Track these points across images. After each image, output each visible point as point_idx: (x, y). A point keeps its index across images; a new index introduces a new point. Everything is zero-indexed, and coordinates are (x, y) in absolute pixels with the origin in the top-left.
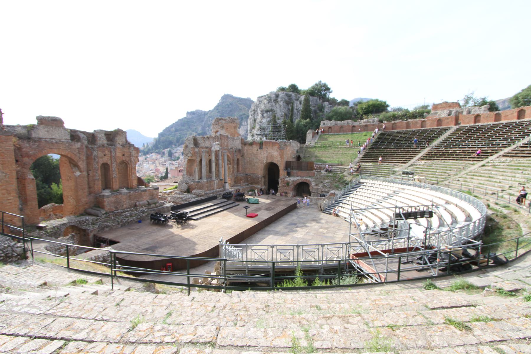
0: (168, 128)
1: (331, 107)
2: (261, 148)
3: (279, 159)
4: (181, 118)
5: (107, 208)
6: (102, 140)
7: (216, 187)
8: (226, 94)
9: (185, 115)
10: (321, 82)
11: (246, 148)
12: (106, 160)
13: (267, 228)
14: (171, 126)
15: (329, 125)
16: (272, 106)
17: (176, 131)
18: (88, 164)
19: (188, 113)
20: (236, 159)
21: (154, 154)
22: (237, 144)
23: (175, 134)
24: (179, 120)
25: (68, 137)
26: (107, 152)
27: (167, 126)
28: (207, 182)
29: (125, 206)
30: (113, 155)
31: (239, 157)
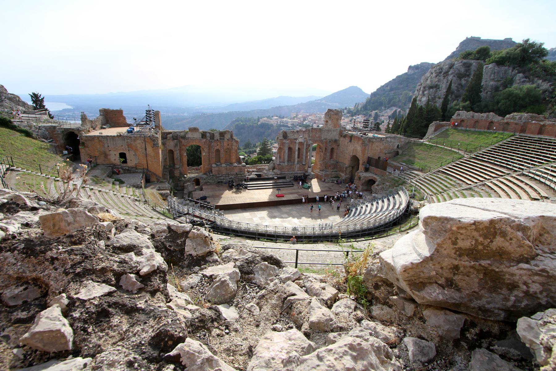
0: (383, 86)
2: (351, 141)
3: (361, 154)
4: (400, 74)
5: (214, 173)
6: (217, 137)
7: (296, 170)
8: (469, 37)
9: (406, 71)
10: (528, 40)
11: (342, 139)
12: (218, 147)
13: (280, 207)
14: (387, 85)
15: (464, 117)
16: (439, 81)
17: (392, 89)
18: (209, 149)
19: (410, 67)
20: (330, 148)
21: (360, 116)
22: (334, 135)
23: (389, 94)
24: (398, 77)
25: (201, 136)
27: (383, 84)
28: (288, 165)
31: (334, 146)
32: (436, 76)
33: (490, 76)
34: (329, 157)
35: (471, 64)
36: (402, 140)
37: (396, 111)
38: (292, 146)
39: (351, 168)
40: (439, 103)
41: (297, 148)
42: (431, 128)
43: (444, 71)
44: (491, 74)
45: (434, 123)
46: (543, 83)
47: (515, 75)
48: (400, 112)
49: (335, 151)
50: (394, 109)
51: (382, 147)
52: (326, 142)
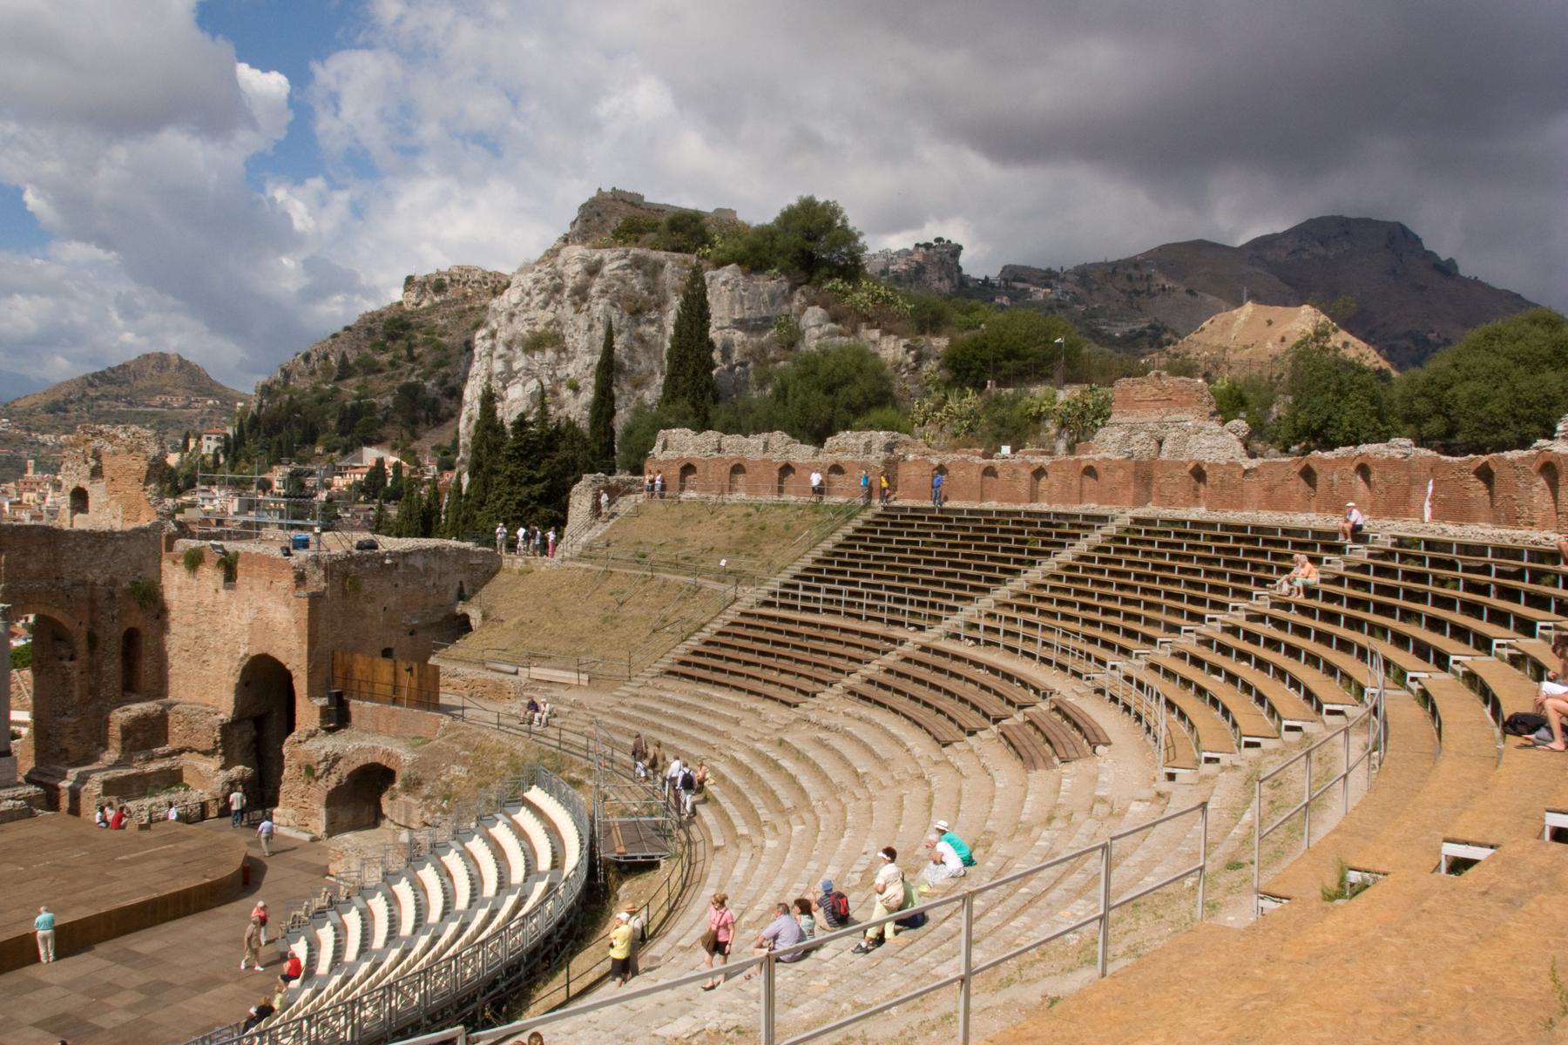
1: (831, 333)
15: (689, 453)
31: (136, 619)
32: (547, 304)
33: (732, 310)
34: (116, 684)
35: (660, 266)
36: (474, 561)
37: (380, 462)
39: (249, 725)
40: (576, 408)
42: (580, 501)
43: (570, 284)
44: (732, 303)
45: (588, 478)
46: (885, 340)
47: (803, 310)
48: (397, 468)
49: (147, 644)
50: (370, 455)
51: (392, 600)
52: (92, 601)
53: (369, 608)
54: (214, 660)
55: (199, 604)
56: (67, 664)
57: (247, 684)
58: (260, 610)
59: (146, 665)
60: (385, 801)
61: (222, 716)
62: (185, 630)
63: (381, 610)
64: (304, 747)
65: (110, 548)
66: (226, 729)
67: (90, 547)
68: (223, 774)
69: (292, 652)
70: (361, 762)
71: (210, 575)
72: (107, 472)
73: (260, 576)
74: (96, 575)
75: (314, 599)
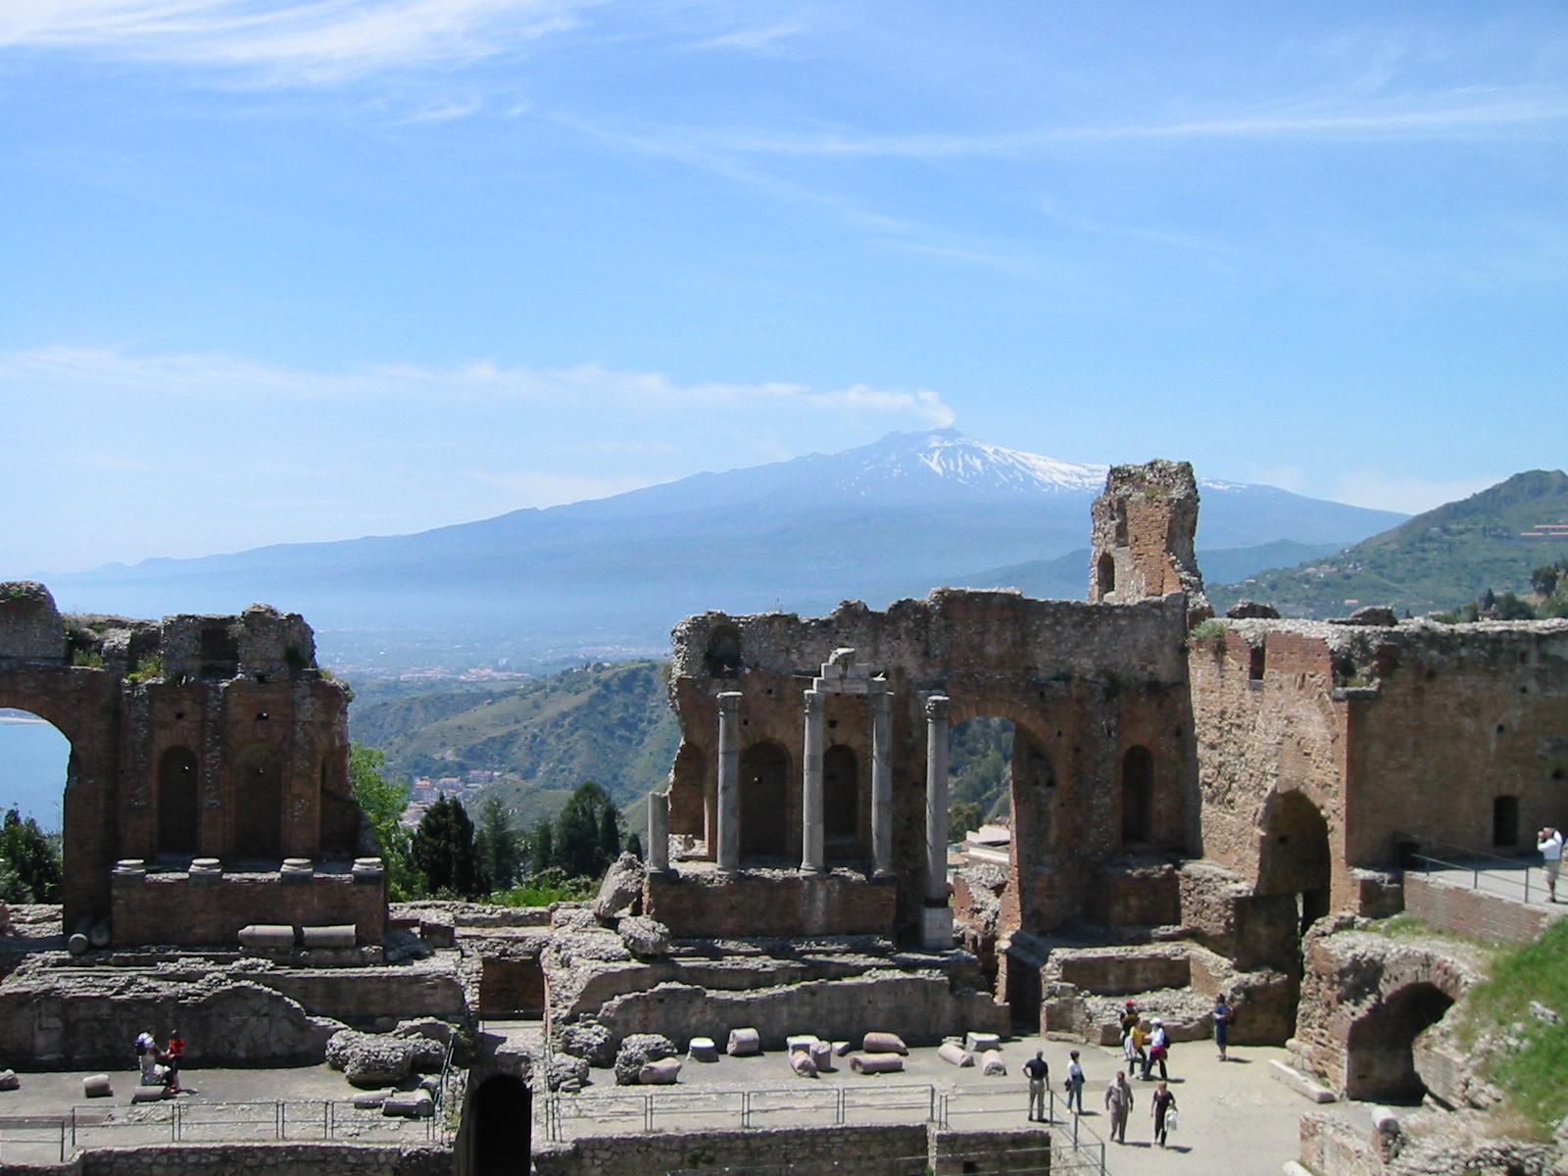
26: (186, 705)
29: (199, 931)
30: (211, 716)
31: (1144, 733)
38: (781, 734)
41: (810, 745)
51: (1514, 716)
53: (1469, 724)
54: (1240, 798)
55: (1223, 713)
56: (1044, 791)
57: (1283, 840)
58: (1289, 720)
59: (1161, 802)
60: (1418, 1053)
61: (1242, 886)
62: (1209, 753)
63: (1492, 730)
64: (1324, 943)
65: (1105, 629)
66: (1241, 906)
67: (1076, 626)
68: (1238, 977)
69: (1329, 792)
70: (1408, 979)
71: (1237, 665)
72: (1131, 528)
73: (1291, 669)
74: (1084, 664)
75: (1358, 704)
